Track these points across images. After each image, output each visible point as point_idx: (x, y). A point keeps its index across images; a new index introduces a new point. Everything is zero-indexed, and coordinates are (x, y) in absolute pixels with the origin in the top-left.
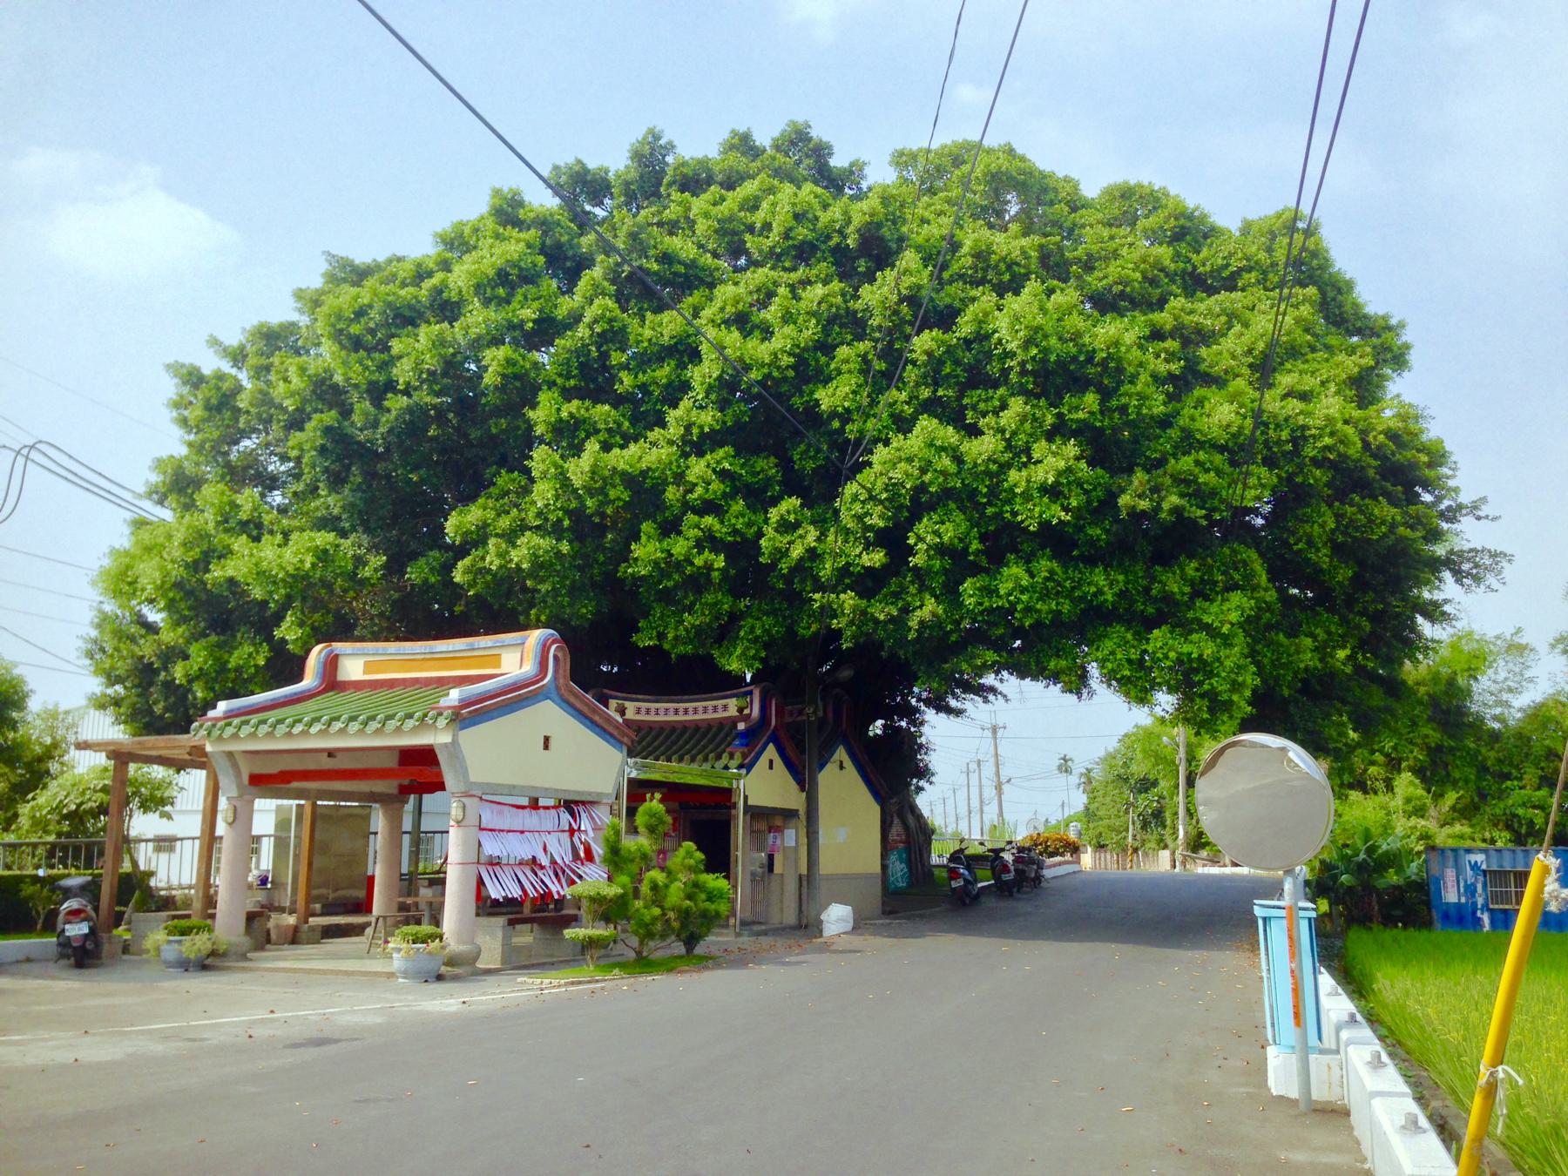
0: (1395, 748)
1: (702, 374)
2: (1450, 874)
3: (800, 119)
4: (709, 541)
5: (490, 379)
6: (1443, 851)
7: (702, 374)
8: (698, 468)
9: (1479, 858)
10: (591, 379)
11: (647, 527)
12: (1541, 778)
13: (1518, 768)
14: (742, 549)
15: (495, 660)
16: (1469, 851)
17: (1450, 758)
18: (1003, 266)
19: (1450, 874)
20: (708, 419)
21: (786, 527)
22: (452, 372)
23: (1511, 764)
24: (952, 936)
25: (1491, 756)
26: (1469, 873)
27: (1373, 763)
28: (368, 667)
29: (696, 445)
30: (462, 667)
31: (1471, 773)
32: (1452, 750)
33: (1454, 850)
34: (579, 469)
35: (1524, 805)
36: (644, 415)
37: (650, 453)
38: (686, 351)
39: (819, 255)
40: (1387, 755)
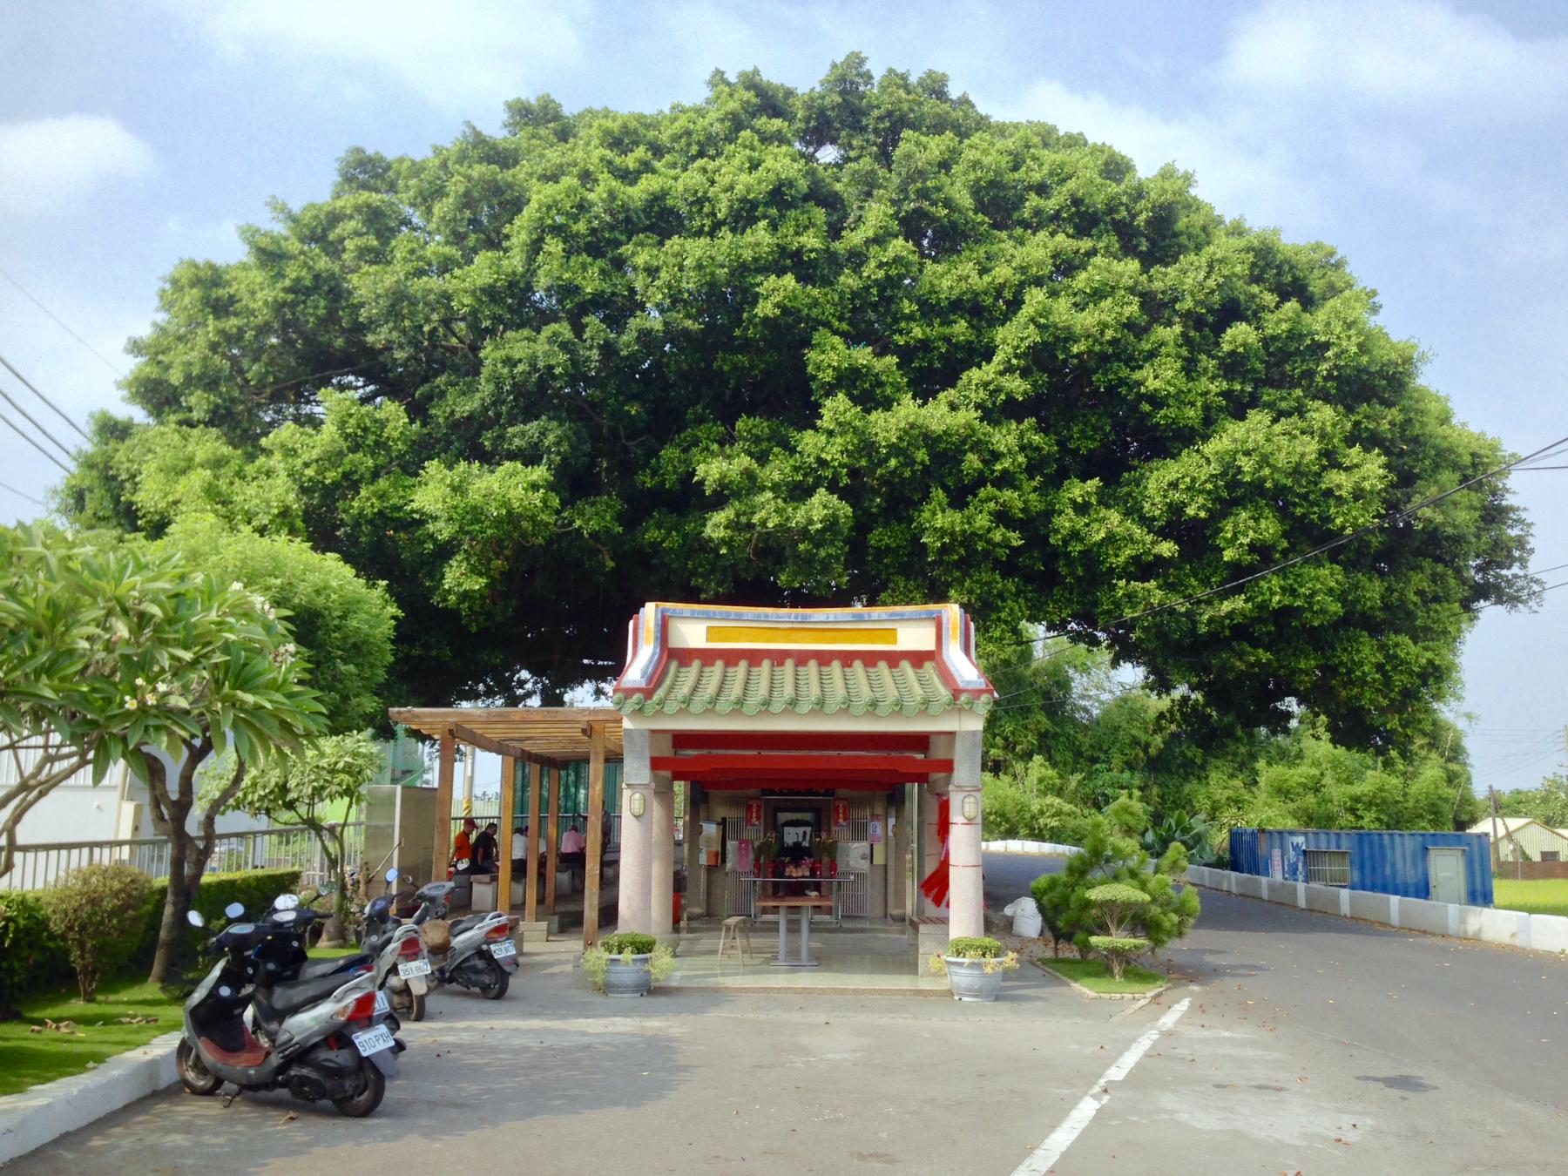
0: (1013, 733)
1: (1011, 336)
2: (1277, 853)
3: (939, 69)
4: (1003, 517)
5: (765, 309)
6: (1270, 833)
7: (1011, 336)
8: (1005, 438)
9: (1300, 840)
10: (868, 318)
11: (939, 494)
12: (1126, 763)
13: (1106, 752)
14: (1034, 526)
15: (891, 635)
16: (1292, 833)
17: (1053, 743)
18: (1286, 268)
19: (1277, 853)
20: (1017, 386)
21: (1082, 508)
22: (725, 297)
23: (1101, 749)
24: (1229, 933)
25: (1085, 741)
26: (1292, 853)
27: (993, 746)
28: (711, 633)
29: (1001, 410)
30: (846, 641)
31: (1069, 756)
32: (1055, 736)
33: (1280, 833)
34: (886, 425)
35: (1112, 785)
36: (932, 373)
37: (940, 415)
38: (983, 311)
39: (1102, 226)
40: (1006, 739)
